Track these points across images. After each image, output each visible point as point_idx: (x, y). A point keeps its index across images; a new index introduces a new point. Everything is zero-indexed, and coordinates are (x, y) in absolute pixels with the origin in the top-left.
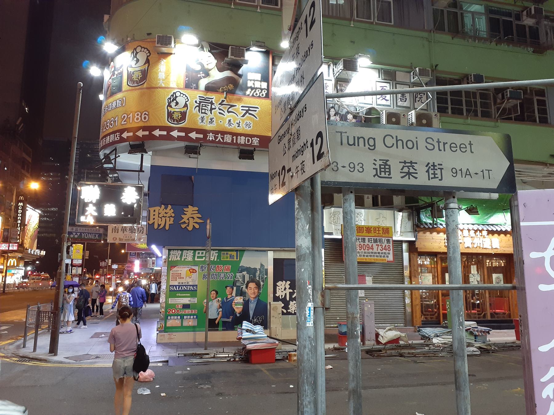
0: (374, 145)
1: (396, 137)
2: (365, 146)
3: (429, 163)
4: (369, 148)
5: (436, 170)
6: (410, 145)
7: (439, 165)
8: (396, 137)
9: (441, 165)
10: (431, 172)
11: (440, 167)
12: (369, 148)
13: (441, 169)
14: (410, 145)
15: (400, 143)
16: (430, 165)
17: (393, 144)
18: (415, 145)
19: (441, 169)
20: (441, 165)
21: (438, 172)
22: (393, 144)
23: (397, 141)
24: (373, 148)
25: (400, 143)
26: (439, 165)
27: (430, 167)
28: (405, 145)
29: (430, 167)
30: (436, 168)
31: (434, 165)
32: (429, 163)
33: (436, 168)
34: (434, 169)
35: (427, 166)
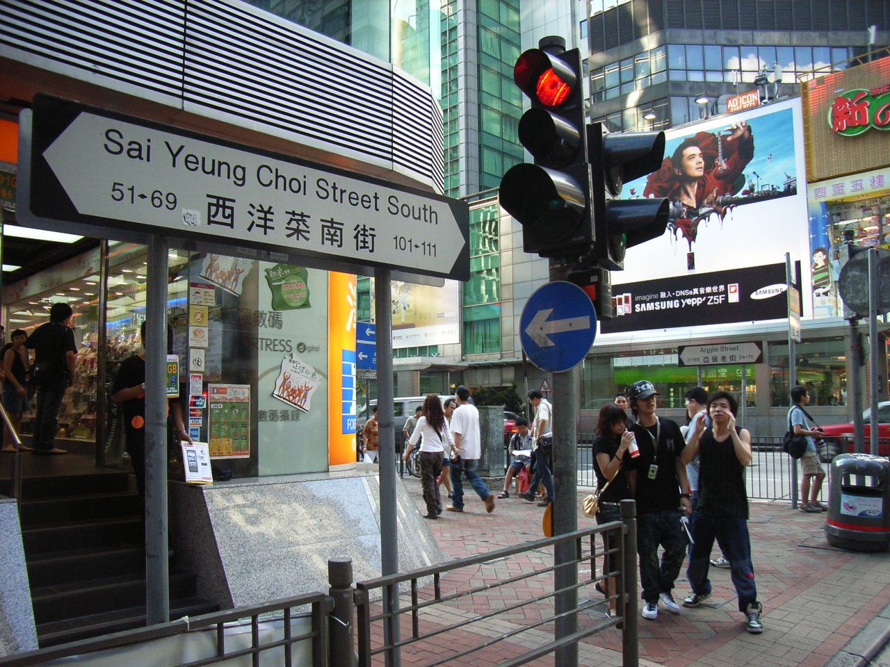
0: (243, 179)
1: (277, 170)
2: (229, 177)
3: (358, 226)
4: (235, 182)
5: (367, 236)
6: (295, 186)
7: (371, 229)
8: (277, 170)
9: (373, 230)
10: (361, 238)
11: (372, 232)
12: (235, 182)
13: (373, 236)
14: (295, 186)
15: (281, 180)
16: (359, 229)
17: (271, 181)
18: (302, 188)
19: (373, 236)
20: (373, 230)
21: (369, 239)
22: (271, 181)
23: (277, 177)
24: (240, 182)
25: (281, 180)
26: (371, 229)
27: (359, 232)
28: (288, 185)
29: (359, 232)
30: (366, 233)
31: (364, 230)
32: (358, 226)
33: (366, 233)
34: (364, 235)
35: (355, 229)
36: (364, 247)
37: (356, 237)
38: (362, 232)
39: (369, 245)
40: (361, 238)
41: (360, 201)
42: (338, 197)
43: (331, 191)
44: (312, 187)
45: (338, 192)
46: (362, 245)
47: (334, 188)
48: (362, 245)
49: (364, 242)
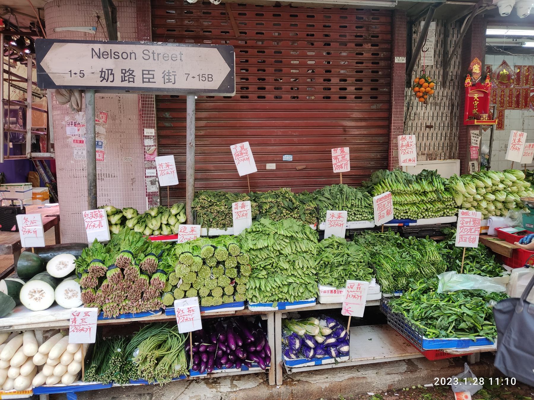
3: (165, 71)
10: (166, 77)
13: (175, 75)
16: (165, 72)
19: (175, 75)
21: (172, 78)
31: (169, 73)
32: (165, 71)
34: (169, 75)
35: (163, 73)
36: (169, 82)
37: (164, 77)
38: (167, 74)
39: (173, 81)
40: (167, 77)
41: (170, 58)
42: (156, 57)
43: (151, 55)
44: (139, 54)
45: (156, 55)
46: (168, 81)
47: (153, 53)
48: (168, 81)
49: (169, 79)
